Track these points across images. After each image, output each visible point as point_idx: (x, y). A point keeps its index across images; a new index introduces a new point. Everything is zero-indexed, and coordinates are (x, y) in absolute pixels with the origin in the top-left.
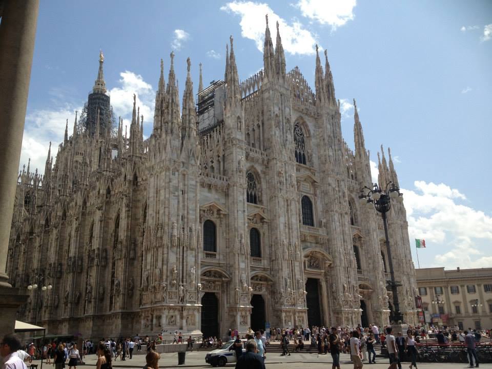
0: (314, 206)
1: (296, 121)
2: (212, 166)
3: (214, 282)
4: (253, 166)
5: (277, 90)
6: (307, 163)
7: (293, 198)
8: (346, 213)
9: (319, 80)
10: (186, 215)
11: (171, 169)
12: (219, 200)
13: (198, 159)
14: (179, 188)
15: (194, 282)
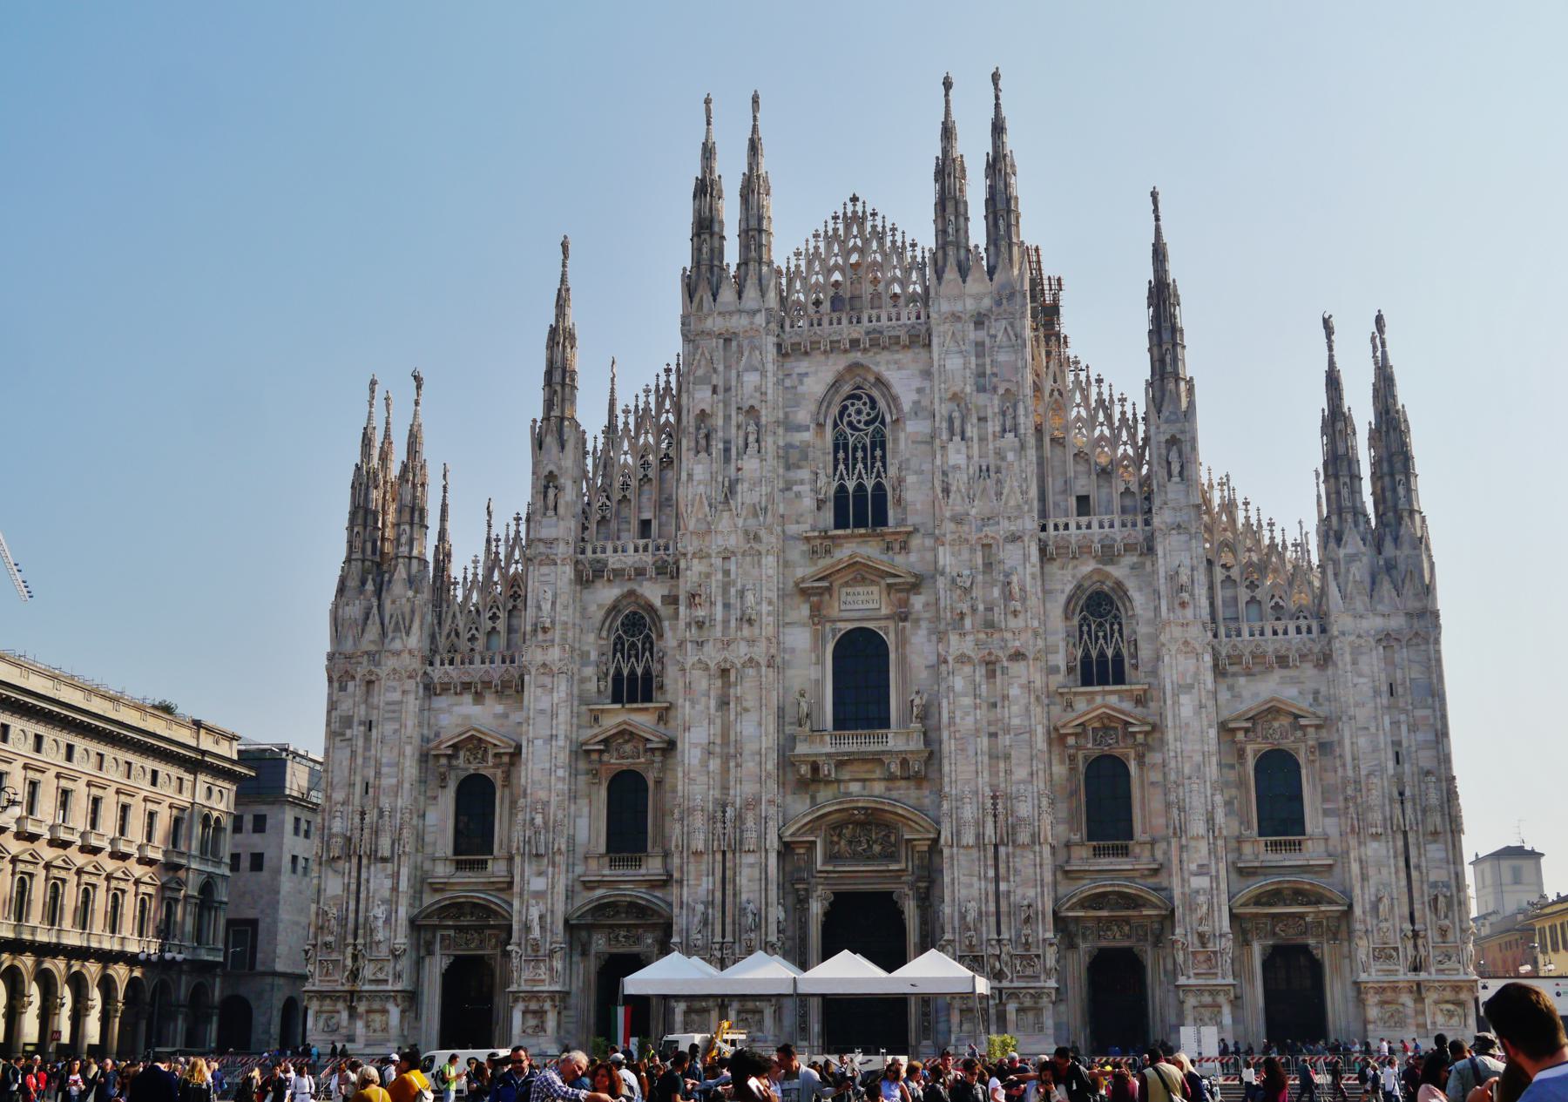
0: (892, 656)
1: (835, 385)
2: (494, 628)
3: (479, 929)
4: (632, 593)
5: (709, 334)
6: (891, 513)
7: (751, 660)
8: (1018, 656)
9: (948, 204)
10: (371, 781)
11: (335, 677)
12: (506, 716)
13: (408, 634)
14: (356, 719)
15: (380, 936)
